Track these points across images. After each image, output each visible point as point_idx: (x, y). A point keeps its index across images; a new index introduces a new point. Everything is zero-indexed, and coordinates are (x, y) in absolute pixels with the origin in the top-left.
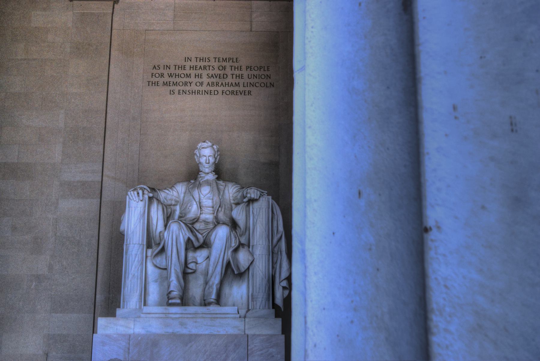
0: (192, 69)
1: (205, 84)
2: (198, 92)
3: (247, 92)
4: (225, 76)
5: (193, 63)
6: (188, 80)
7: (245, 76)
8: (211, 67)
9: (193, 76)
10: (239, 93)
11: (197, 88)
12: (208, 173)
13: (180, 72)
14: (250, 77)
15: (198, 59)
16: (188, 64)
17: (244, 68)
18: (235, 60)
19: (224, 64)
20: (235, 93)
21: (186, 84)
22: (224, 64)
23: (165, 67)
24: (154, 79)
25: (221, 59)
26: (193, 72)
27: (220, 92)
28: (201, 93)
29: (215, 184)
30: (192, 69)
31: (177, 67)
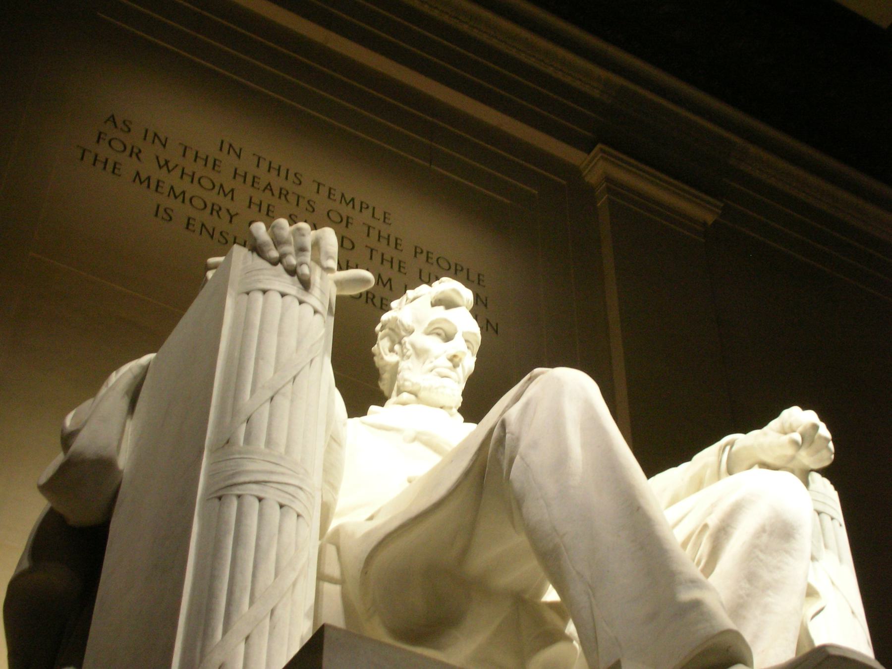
6: (224, 202)
13: (198, 168)
15: (264, 165)
18: (379, 214)
19: (346, 210)
21: (215, 210)
22: (346, 210)
25: (338, 197)
31: (190, 155)
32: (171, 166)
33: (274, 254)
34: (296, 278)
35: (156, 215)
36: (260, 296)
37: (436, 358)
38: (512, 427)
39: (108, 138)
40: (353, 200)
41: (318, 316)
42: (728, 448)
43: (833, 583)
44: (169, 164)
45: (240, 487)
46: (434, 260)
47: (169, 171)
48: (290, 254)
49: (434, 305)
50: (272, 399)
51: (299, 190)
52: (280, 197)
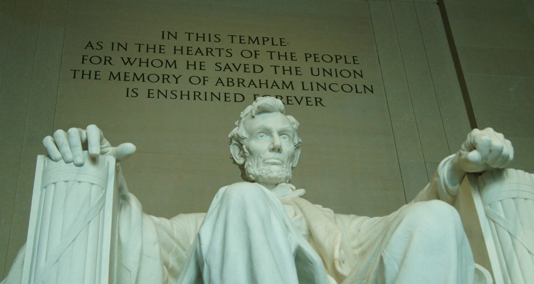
4: (258, 69)
5: (182, 41)
8: (223, 53)
10: (294, 101)
11: (192, 88)
12: (277, 185)
13: (151, 56)
14: (315, 73)
16: (169, 44)
17: (300, 56)
18: (277, 41)
19: (253, 47)
21: (165, 78)
23: (116, 46)
24: (88, 67)
26: (182, 60)
28: (202, 96)
29: (305, 203)
31: (144, 48)
32: (132, 61)
35: (127, 96)
39: (89, 58)
40: (257, 38)
44: (131, 60)
46: (320, 59)
47: (131, 65)
51: (219, 45)
52: (207, 55)
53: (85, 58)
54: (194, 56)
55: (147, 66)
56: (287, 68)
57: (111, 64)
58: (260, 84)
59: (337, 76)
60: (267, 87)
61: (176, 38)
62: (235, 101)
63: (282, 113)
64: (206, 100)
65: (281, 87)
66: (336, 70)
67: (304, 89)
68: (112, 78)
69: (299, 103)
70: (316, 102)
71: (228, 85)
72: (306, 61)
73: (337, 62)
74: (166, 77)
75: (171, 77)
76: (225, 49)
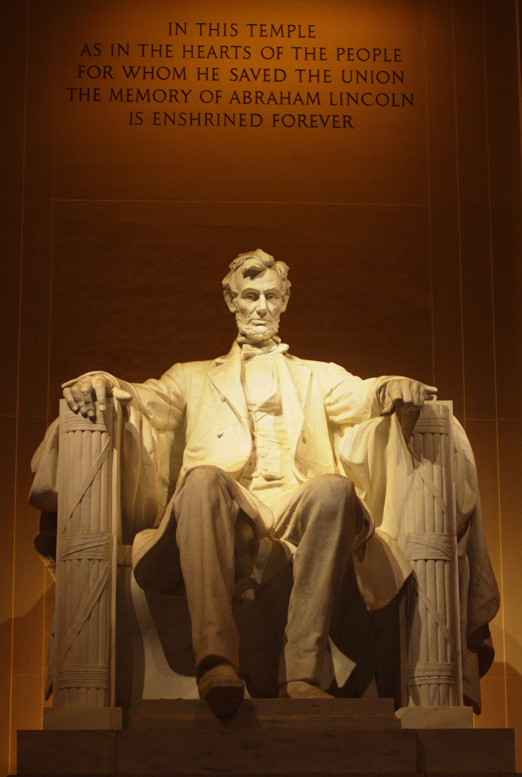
0: (188, 55)
1: (227, 96)
2: (208, 118)
3: (341, 119)
5: (192, 38)
6: (179, 84)
7: (335, 75)
9: (192, 74)
10: (319, 122)
14: (347, 79)
15: (206, 29)
17: (331, 53)
18: (305, 32)
19: (276, 41)
20: (308, 121)
21: (173, 95)
23: (116, 47)
25: (268, 28)
26: (192, 65)
27: (268, 120)
28: (215, 120)
30: (188, 55)
31: (148, 49)
32: (135, 70)
33: (75, 408)
34: (88, 418)
35: (131, 123)
36: (71, 433)
37: (251, 313)
38: (176, 510)
39: (86, 69)
41: (104, 434)
42: (383, 389)
43: (424, 481)
45: (70, 556)
46: (355, 56)
47: (135, 76)
48: (82, 407)
49: (245, 276)
50: (81, 500)
51: (235, 41)
52: (221, 57)
53: (82, 69)
54: (205, 59)
55: (153, 78)
56: (314, 73)
57: (112, 77)
58: (282, 98)
59: (372, 82)
60: (289, 103)
61: (185, 32)
62: (252, 125)
63: (270, 267)
64: (219, 125)
65: (305, 100)
66: (372, 71)
67: (331, 104)
68: (113, 98)
69: (325, 125)
70: (345, 122)
71: (245, 103)
72: (338, 60)
73: (374, 60)
74: (174, 93)
75: (180, 92)
76: (243, 48)
